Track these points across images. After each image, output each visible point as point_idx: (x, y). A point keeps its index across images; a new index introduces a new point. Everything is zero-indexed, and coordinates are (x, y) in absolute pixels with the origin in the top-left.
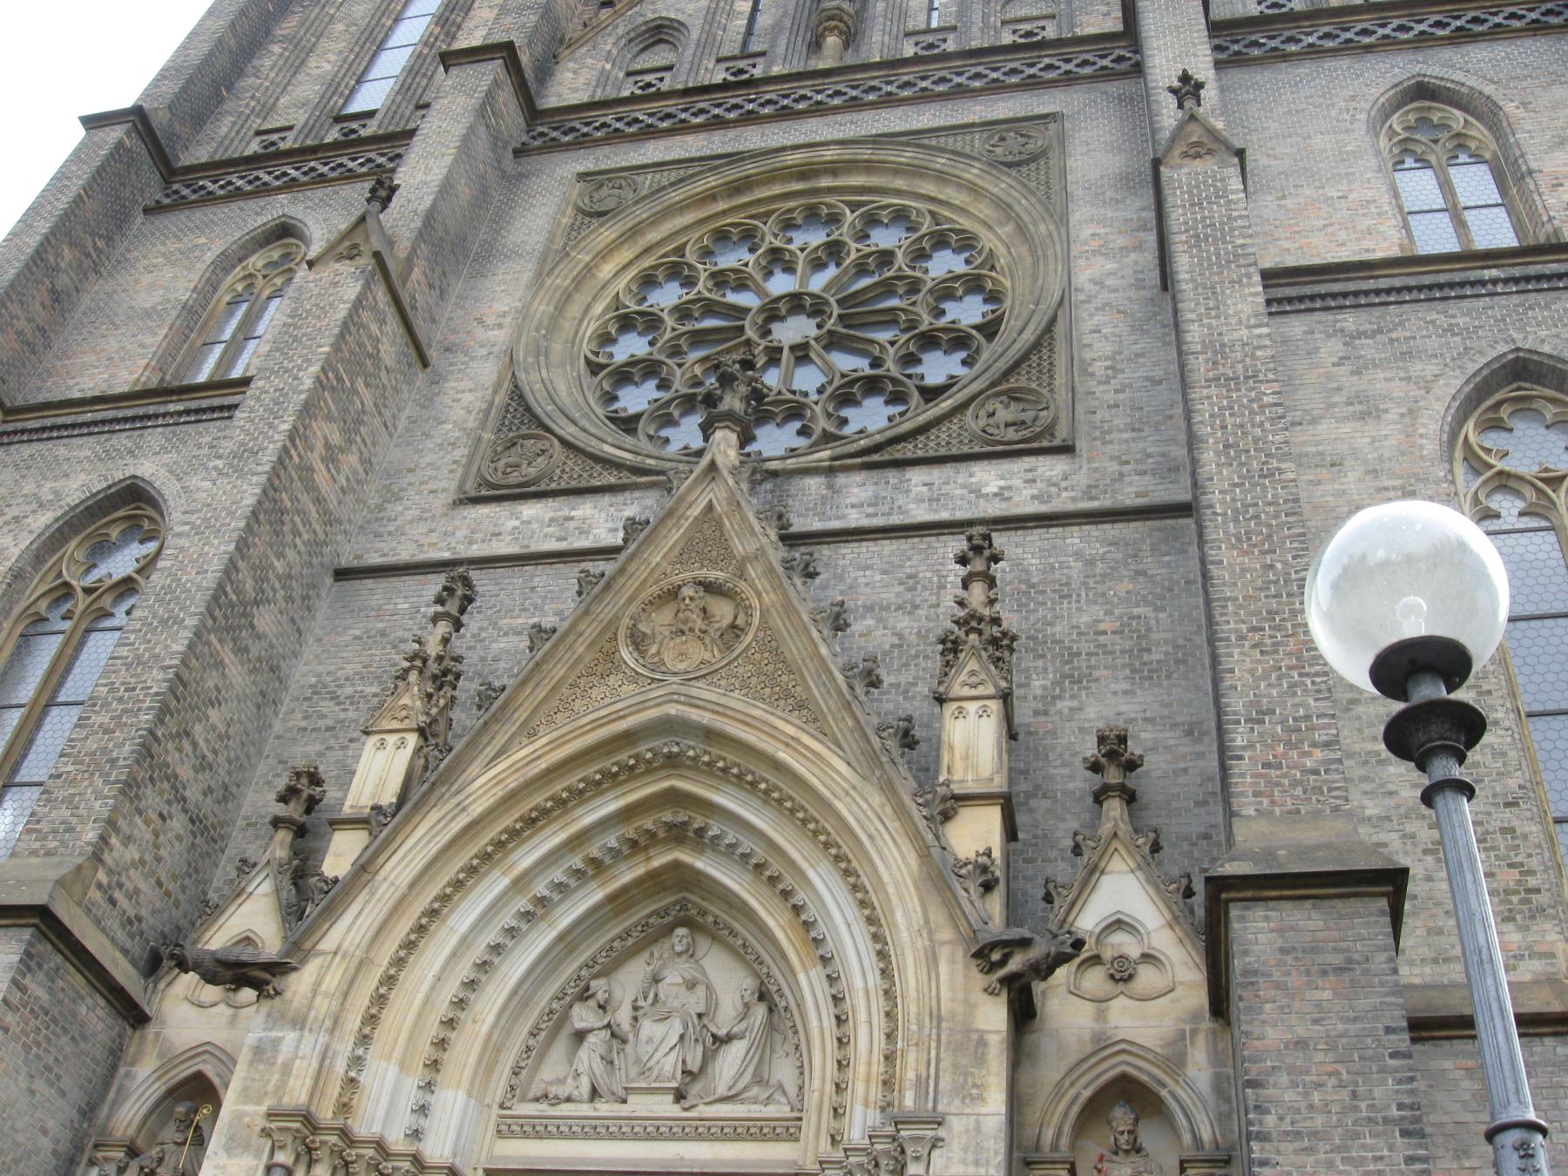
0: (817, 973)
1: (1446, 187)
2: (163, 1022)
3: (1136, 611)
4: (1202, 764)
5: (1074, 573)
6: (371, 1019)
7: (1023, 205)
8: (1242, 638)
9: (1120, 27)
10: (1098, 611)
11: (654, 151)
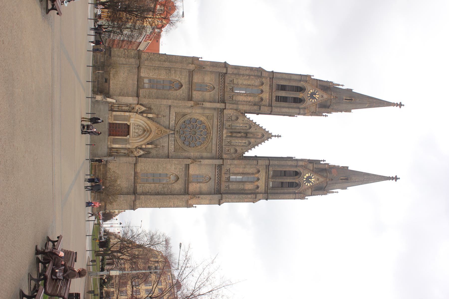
7: (201, 149)
10: (161, 152)
11: (215, 120)
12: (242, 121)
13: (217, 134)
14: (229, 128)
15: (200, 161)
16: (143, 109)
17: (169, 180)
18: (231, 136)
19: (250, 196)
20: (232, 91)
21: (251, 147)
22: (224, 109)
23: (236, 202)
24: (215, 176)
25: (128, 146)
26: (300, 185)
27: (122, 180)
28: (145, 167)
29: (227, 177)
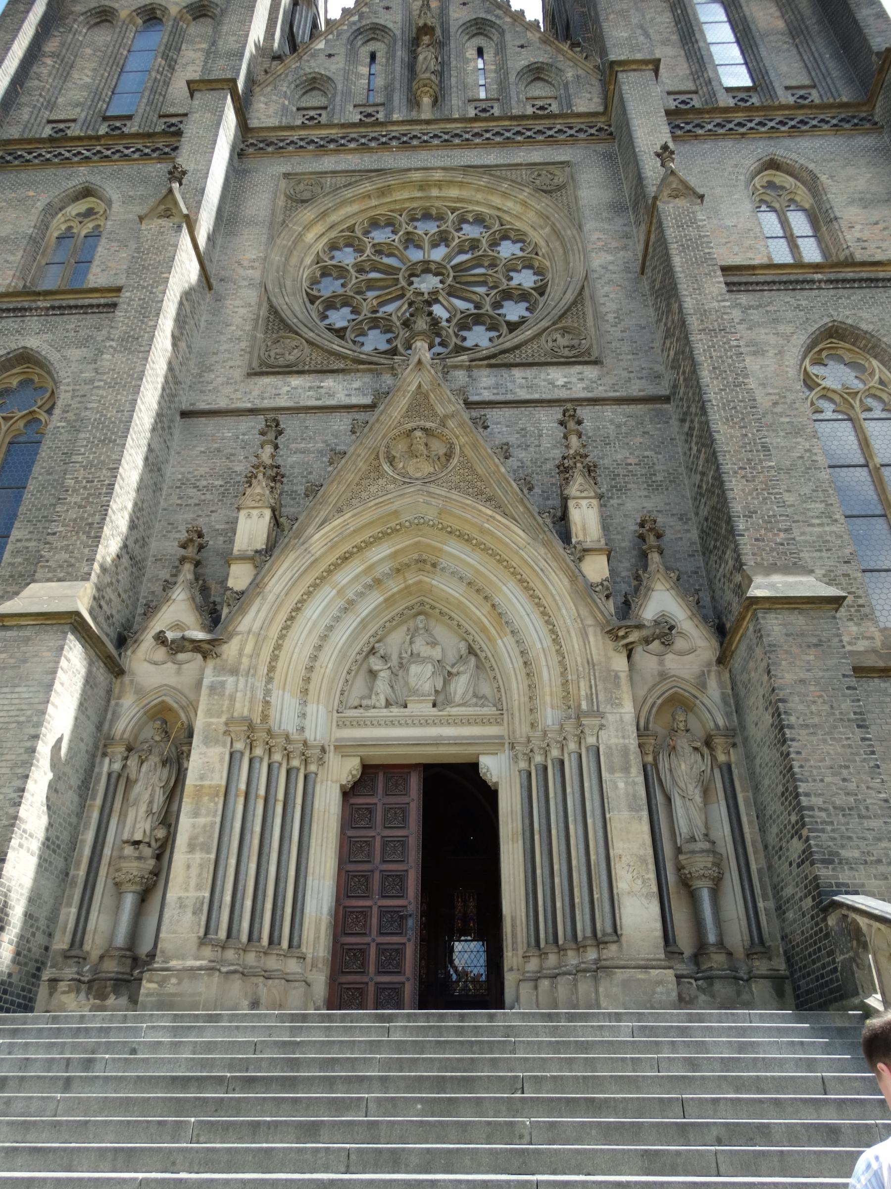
0: (509, 640)
1: (785, 223)
2: (133, 674)
3: (646, 453)
4: (689, 535)
5: (610, 431)
6: (272, 669)
8: (735, 473)
9: (601, 109)
11: (328, 163)
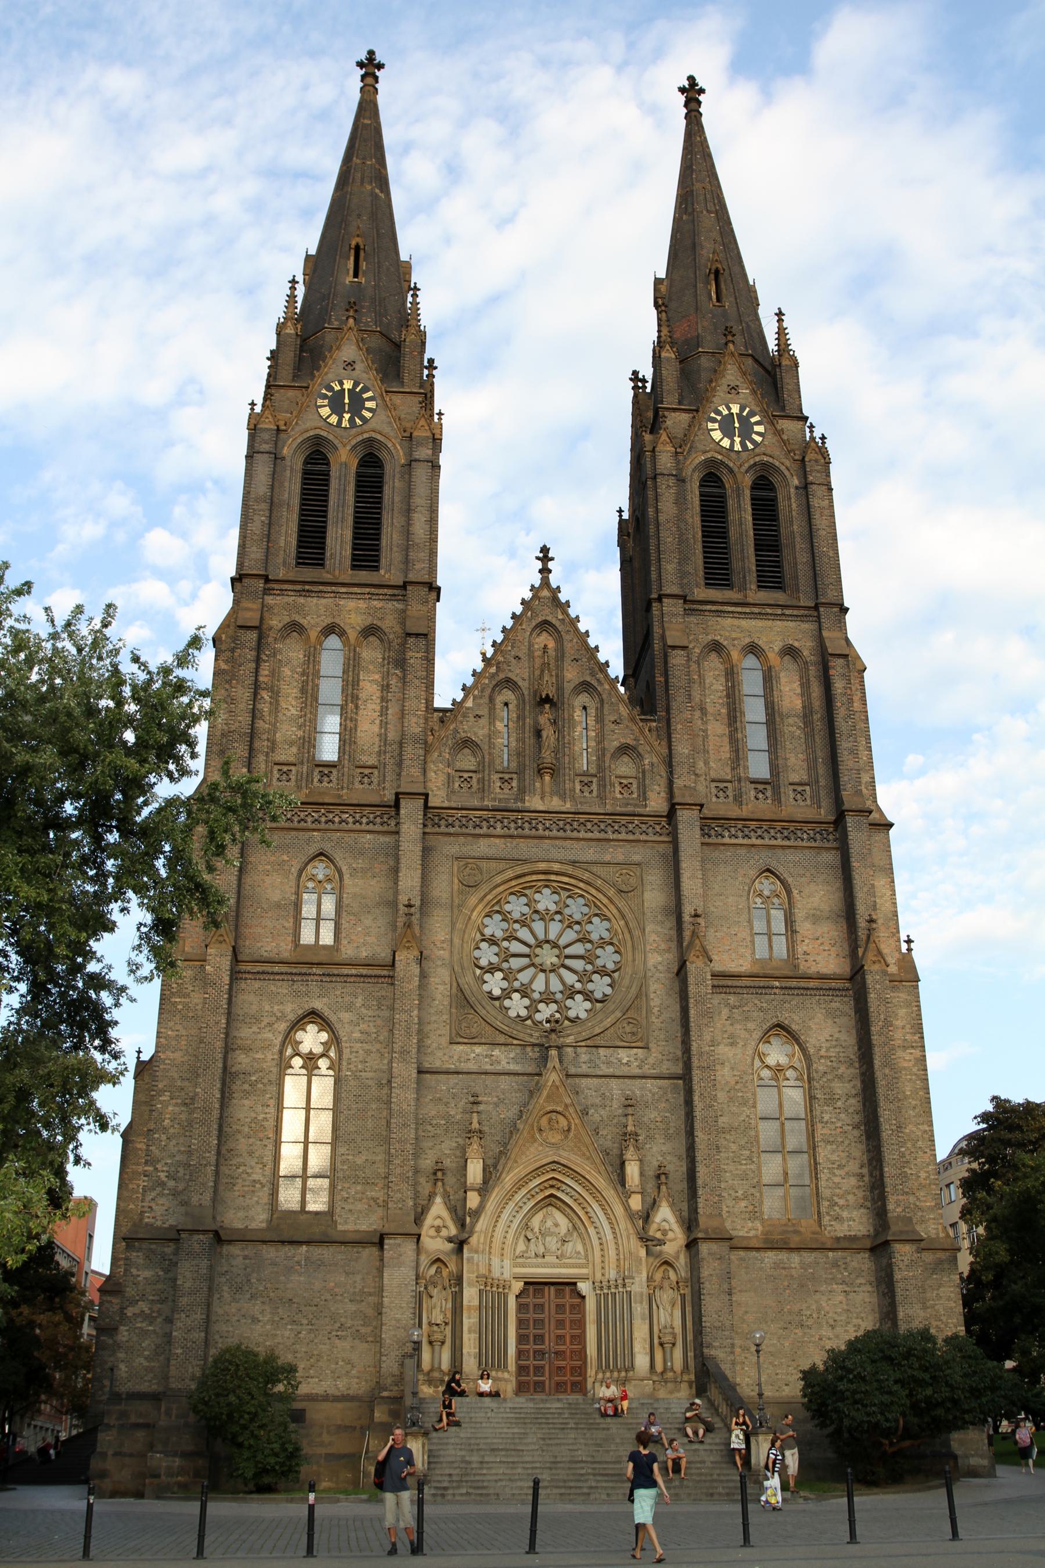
6: (490, 1247)
7: (629, 916)
11: (483, 847)
12: (483, 721)
13: (549, 838)
14: (514, 784)
15: (696, 916)
16: (438, 1209)
17: (790, 1073)
18: (554, 771)
19: (838, 685)
20: (335, 771)
21: (602, 680)
22: (426, 806)
23: (870, 749)
24: (753, 845)
25: (638, 1285)
26: (766, 466)
27: (809, 1313)
28: (733, 1194)
29: (753, 793)
